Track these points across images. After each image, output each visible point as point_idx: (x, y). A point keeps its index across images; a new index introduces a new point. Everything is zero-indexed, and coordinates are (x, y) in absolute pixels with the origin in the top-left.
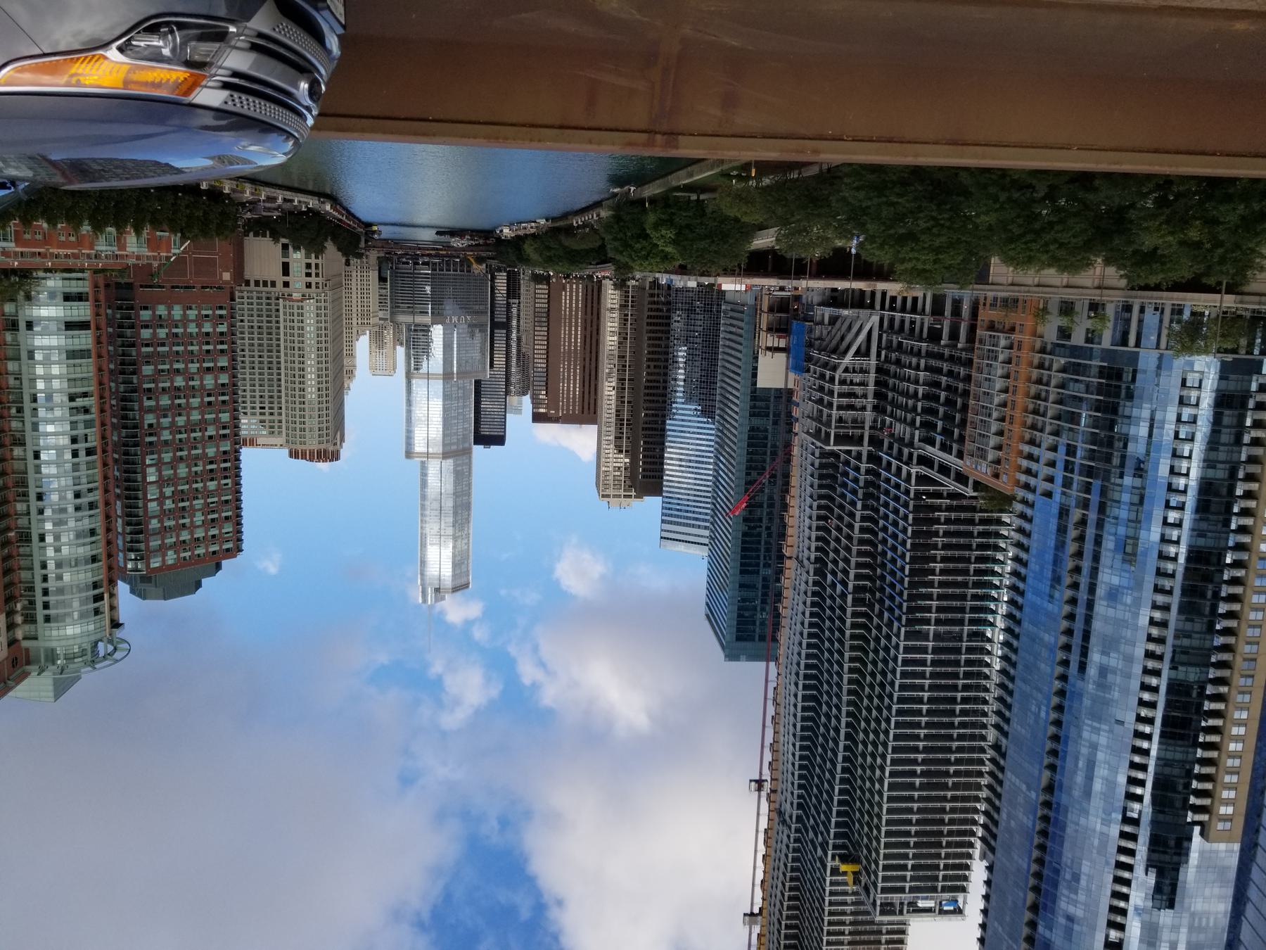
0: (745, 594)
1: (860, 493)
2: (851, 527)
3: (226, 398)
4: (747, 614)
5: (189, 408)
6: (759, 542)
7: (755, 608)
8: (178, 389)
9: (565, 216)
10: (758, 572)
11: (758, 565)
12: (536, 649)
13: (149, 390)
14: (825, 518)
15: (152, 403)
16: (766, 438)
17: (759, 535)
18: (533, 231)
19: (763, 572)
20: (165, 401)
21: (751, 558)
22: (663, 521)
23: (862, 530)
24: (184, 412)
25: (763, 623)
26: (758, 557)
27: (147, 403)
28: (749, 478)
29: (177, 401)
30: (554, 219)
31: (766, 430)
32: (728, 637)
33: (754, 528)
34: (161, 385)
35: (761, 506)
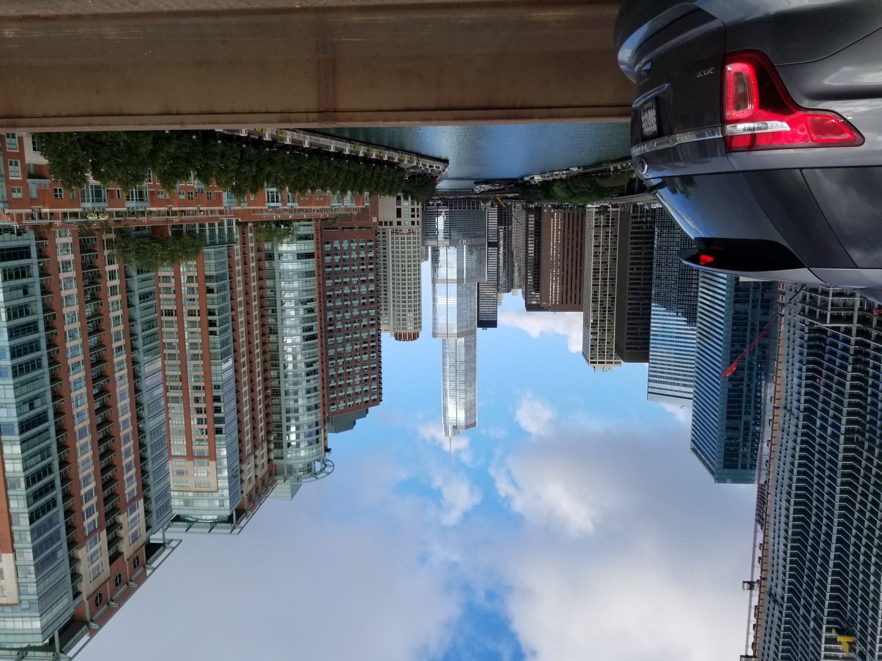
0: (730, 434)
1: (851, 359)
2: (843, 385)
3: (373, 300)
4: (732, 448)
5: (352, 307)
6: (741, 396)
7: (738, 444)
8: (346, 295)
9: (598, 164)
10: (740, 418)
11: (740, 413)
12: (509, 473)
13: (330, 296)
14: (813, 378)
15: (331, 304)
16: (746, 319)
17: (741, 390)
18: (564, 177)
19: (744, 418)
20: (339, 303)
21: (734, 407)
22: (649, 381)
23: (852, 387)
24: (349, 310)
25: (744, 456)
26: (740, 407)
27: (329, 305)
28: (733, 349)
29: (346, 303)
30: (585, 167)
31: (747, 313)
32: (717, 466)
33: (738, 385)
34: (336, 292)
35: (743, 369)
